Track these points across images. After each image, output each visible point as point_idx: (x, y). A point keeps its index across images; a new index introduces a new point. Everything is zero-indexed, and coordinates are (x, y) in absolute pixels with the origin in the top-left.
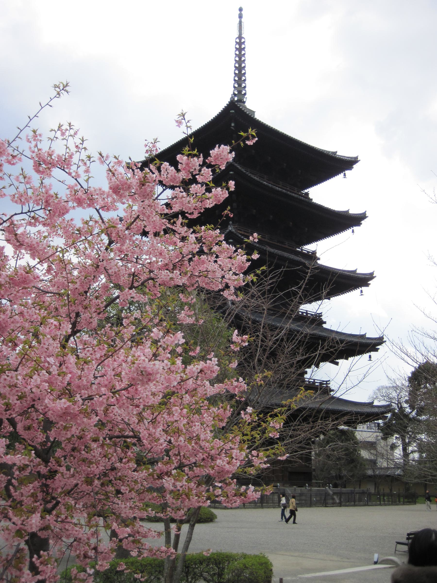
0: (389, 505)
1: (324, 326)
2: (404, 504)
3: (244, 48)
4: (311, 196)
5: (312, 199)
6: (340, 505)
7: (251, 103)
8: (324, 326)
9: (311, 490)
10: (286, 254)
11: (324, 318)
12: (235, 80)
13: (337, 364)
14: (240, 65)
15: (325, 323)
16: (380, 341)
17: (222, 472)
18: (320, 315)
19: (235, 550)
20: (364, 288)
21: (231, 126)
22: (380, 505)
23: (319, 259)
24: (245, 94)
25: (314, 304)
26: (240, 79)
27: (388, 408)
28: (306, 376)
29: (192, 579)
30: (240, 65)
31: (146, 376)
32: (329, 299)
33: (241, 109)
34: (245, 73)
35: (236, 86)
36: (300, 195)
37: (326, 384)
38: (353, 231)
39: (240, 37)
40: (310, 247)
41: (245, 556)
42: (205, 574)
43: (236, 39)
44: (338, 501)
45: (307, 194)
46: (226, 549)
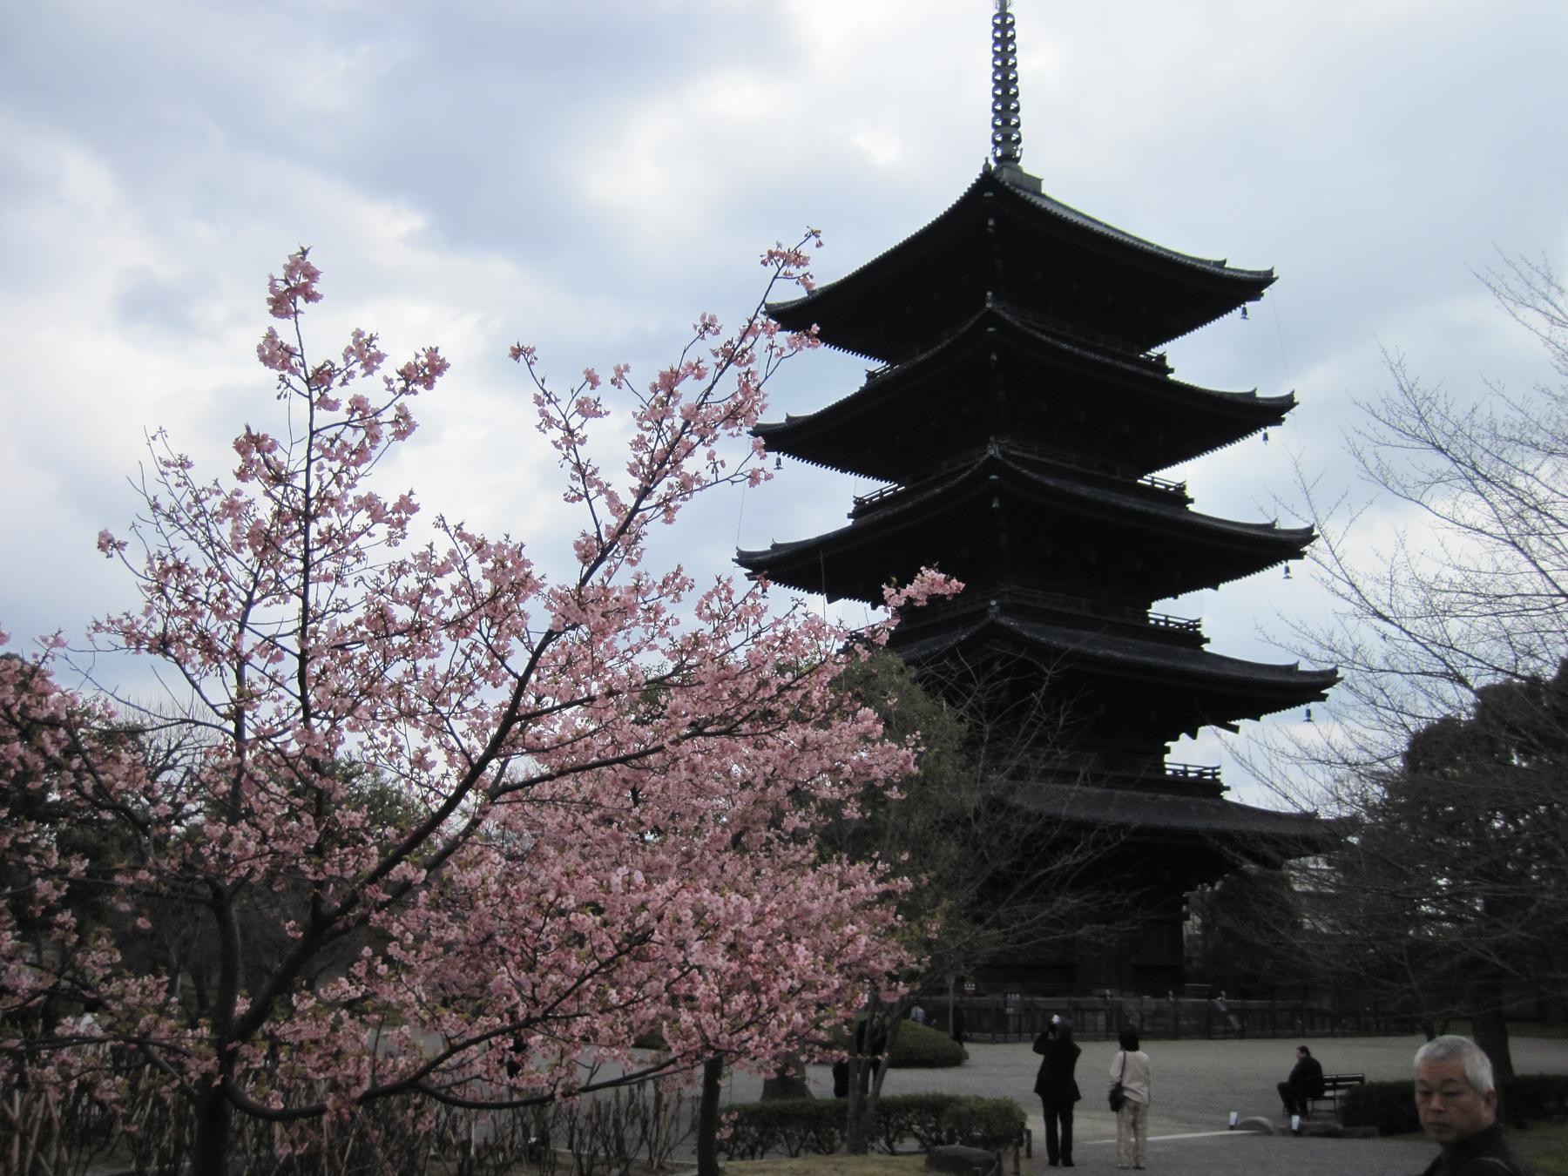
0: (1352, 1035)
1: (1206, 647)
2: (1388, 1033)
3: (1013, 37)
4: (1169, 363)
5: (1172, 371)
6: (1242, 1035)
7: (1029, 164)
8: (1206, 647)
9: (1176, 1004)
10: (1115, 498)
11: (1204, 631)
12: (994, 126)
13: (1235, 729)
14: (1005, 77)
15: (1207, 641)
16: (1330, 678)
17: (873, 970)
18: (1196, 624)
19: (962, 1094)
20: (1291, 563)
21: (986, 225)
22: (1333, 1035)
23: (1191, 501)
24: (1018, 141)
25: (1184, 598)
26: (1006, 107)
27: (1351, 824)
28: (1167, 758)
29: (897, 1133)
30: (1005, 77)
31: (808, 912)
32: (1216, 588)
33: (1007, 189)
34: (1016, 95)
35: (999, 123)
36: (1148, 363)
37: (1214, 774)
38: (1266, 437)
39: (1003, 13)
40: (1167, 476)
41: (979, 1099)
42: (916, 1127)
43: (995, 17)
44: (1237, 1026)
45: (1162, 358)
46: (947, 1091)
